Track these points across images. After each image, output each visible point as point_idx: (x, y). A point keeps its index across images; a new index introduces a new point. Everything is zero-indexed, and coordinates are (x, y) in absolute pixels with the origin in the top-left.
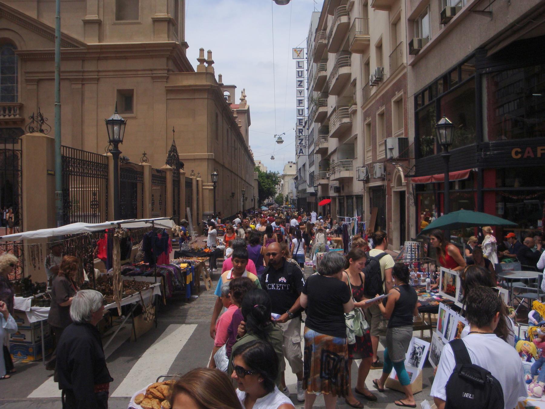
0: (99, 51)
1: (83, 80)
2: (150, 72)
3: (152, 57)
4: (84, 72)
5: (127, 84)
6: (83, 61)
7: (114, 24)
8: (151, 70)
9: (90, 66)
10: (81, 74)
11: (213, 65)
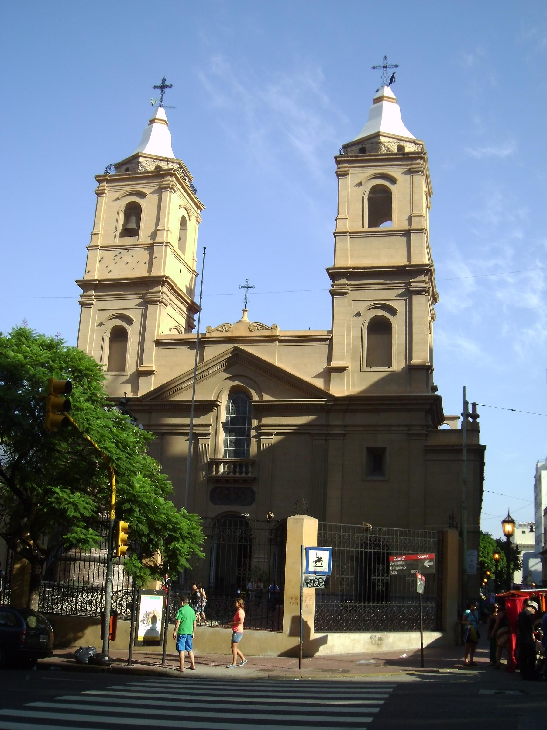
1: (327, 435)
2: (406, 428)
4: (328, 426)
8: (407, 426)
11: (478, 420)
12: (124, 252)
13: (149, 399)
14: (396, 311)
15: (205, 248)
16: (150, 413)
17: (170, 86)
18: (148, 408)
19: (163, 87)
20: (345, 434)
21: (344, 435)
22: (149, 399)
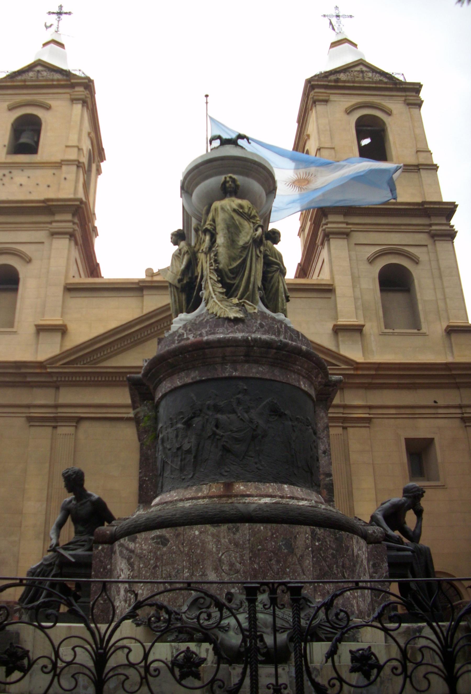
0: (373, 372)
1: (345, 420)
3: (458, 386)
7: (383, 334)
10: (341, 410)
13: (58, 365)
14: (418, 258)
15: (207, 96)
16: (57, 388)
18: (55, 379)
21: (369, 420)
22: (58, 365)
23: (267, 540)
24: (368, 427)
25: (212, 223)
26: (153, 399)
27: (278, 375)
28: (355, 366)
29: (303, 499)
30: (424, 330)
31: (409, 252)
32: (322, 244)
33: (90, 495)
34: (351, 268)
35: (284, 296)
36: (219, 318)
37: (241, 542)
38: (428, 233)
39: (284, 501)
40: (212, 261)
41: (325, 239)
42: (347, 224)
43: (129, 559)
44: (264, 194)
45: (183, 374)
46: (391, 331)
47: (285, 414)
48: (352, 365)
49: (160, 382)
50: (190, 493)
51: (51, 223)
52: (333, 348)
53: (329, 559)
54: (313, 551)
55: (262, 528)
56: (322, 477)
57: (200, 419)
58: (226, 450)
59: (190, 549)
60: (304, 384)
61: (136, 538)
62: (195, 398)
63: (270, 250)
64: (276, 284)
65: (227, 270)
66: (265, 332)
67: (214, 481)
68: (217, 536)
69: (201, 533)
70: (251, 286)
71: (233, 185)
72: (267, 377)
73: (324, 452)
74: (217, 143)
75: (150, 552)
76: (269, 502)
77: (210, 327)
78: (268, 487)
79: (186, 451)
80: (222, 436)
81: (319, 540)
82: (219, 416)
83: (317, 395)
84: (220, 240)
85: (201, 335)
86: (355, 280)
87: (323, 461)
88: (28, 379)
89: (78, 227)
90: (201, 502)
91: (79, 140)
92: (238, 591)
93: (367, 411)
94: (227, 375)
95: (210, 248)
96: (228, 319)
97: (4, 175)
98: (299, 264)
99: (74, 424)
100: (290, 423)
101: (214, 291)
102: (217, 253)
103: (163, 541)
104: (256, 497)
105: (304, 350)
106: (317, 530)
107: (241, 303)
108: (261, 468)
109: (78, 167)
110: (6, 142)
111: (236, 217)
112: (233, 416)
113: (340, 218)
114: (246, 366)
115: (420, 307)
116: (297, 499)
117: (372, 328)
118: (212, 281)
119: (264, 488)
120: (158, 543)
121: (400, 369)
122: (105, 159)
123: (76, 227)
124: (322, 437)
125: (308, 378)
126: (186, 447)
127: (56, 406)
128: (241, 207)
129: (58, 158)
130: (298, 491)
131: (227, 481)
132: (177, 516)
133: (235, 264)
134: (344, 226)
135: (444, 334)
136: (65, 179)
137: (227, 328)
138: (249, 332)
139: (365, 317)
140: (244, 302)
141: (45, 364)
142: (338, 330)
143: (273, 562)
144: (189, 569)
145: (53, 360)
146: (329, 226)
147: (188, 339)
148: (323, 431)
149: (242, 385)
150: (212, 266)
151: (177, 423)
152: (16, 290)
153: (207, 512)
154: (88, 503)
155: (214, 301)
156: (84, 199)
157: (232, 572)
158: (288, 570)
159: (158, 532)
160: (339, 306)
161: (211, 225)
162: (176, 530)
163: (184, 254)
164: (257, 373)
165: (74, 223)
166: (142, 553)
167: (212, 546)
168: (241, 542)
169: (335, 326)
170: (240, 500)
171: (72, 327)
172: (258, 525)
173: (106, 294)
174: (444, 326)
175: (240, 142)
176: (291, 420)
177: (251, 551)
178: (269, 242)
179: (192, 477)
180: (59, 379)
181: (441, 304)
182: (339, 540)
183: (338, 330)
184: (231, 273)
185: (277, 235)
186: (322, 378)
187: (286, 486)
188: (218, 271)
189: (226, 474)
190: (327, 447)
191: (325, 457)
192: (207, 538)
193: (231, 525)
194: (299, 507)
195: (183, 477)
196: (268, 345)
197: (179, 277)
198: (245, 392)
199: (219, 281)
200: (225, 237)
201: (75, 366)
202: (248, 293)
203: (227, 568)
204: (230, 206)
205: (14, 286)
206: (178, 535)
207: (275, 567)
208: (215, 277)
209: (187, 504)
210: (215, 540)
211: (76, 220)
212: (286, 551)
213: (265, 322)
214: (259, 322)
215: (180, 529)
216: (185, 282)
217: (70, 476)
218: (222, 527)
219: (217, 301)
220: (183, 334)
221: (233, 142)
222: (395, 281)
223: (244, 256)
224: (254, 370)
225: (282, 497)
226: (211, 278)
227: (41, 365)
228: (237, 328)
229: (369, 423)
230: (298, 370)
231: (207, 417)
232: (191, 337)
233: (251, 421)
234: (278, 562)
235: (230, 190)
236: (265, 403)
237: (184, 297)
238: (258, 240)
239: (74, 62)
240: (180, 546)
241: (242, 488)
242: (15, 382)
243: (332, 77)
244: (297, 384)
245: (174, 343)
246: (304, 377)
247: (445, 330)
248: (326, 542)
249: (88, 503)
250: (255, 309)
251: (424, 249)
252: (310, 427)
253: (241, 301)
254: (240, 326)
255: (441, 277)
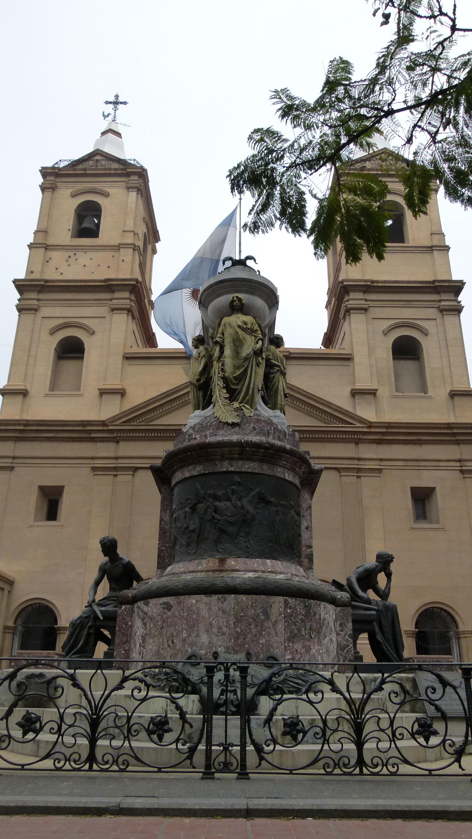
0: (384, 430)
1: (359, 470)
2: (458, 464)
4: (359, 459)
5: (425, 480)
6: (357, 443)
8: (460, 461)
9: (368, 451)
10: (356, 462)
12: (80, 255)
13: (118, 423)
14: (427, 331)
16: (118, 442)
17: (125, 103)
18: (115, 435)
19: (116, 103)
20: (381, 469)
21: (380, 470)
22: (118, 423)
23: (248, 608)
24: (379, 477)
25: (221, 336)
26: (170, 483)
27: (266, 469)
28: (369, 424)
29: (280, 573)
30: (430, 393)
31: (418, 325)
32: (344, 318)
33: (121, 559)
34: (368, 339)
35: (282, 393)
36: (220, 422)
37: (228, 610)
38: (438, 308)
39: (264, 575)
40: (220, 370)
41: (347, 314)
42: (366, 300)
43: (143, 620)
44: (267, 308)
45: (191, 467)
46: (401, 394)
47: (271, 502)
48: (366, 424)
49: (174, 472)
50: (192, 566)
51: (111, 300)
52: (350, 409)
53: (298, 624)
54: (285, 617)
55: (244, 598)
56: (304, 548)
57: (203, 505)
58: (222, 531)
59: (188, 614)
60: (289, 475)
61: (149, 602)
62: (199, 487)
63: (272, 354)
64: (277, 384)
65: (231, 377)
66: (258, 434)
67: (212, 556)
68: (209, 604)
69: (197, 601)
70: (250, 392)
71: (239, 304)
72: (257, 471)
73: (307, 528)
74: (229, 263)
75: (159, 615)
76: (252, 576)
77: (213, 430)
78: (254, 562)
79: (191, 531)
80: (219, 520)
81: (290, 608)
82: (217, 503)
83: (301, 483)
84: (228, 352)
85: (205, 436)
86: (371, 350)
87: (305, 535)
88: (93, 435)
89: (135, 304)
90: (199, 575)
91: (135, 225)
92: (224, 650)
93: (378, 463)
94: (225, 470)
95: (219, 358)
96: (227, 423)
97: (70, 257)
98: (325, 334)
99: (132, 473)
100: (275, 509)
101: (220, 395)
102: (224, 363)
103: (168, 607)
104: (242, 571)
105: (288, 449)
106: (289, 600)
107: (241, 407)
108: (249, 546)
109: (134, 250)
110: (71, 228)
111: (240, 332)
112: (228, 504)
113: (360, 295)
114: (240, 463)
115: (428, 373)
116: (276, 573)
117: (384, 392)
118: (219, 387)
119: (250, 564)
120: (164, 608)
121: (407, 428)
122: (160, 240)
123: (134, 305)
124: (305, 515)
125: (292, 469)
126: (192, 527)
127: (116, 458)
128: (245, 323)
129: (116, 242)
130: (279, 565)
131: (222, 556)
132: (180, 587)
133: (238, 372)
134: (363, 302)
135: (448, 397)
136: (123, 260)
137: (226, 431)
138: (244, 434)
139: (378, 382)
140: (244, 406)
141: (106, 422)
142: (355, 393)
143: (252, 626)
144: (187, 631)
145: (114, 419)
146: (351, 302)
147: (196, 438)
148: (307, 511)
149: (237, 478)
150: (219, 374)
151: (185, 507)
152: (82, 358)
153: (202, 584)
154: (120, 565)
155: (219, 405)
156: (140, 279)
157: (219, 634)
158: (264, 633)
159: (164, 600)
160: (356, 373)
161: (220, 338)
162: (178, 598)
163: (202, 358)
164: (249, 468)
165: (131, 300)
166: (152, 616)
167: (204, 613)
168: (228, 610)
169: (352, 390)
170: (229, 574)
171: (129, 391)
172: (242, 596)
173: (159, 362)
174: (448, 392)
175: (249, 263)
176: (276, 506)
177: (236, 618)
178: (273, 347)
179: (195, 552)
180: (119, 435)
181: (447, 371)
182: (308, 607)
183: (355, 393)
184: (235, 380)
185: (280, 340)
186: (305, 469)
187: (268, 561)
188: (225, 379)
189: (221, 551)
190: (309, 524)
191: (307, 532)
192: (202, 606)
193: (220, 596)
194: (276, 581)
195: (189, 552)
196: (258, 446)
197: (197, 377)
198: (239, 484)
199: (224, 387)
200: (231, 349)
201: (132, 424)
202: (248, 397)
203: (216, 631)
204: (236, 322)
205: (80, 355)
206: (179, 603)
207: (254, 631)
208: (221, 384)
209: (189, 577)
210: (207, 608)
211: (133, 298)
212: (263, 617)
213: (257, 426)
214: (252, 426)
215: (182, 598)
216: (202, 382)
217: (105, 543)
218: (213, 597)
219: (221, 406)
220: (192, 434)
221: (242, 263)
222: (406, 350)
223: (246, 365)
224: (246, 466)
225: (263, 572)
226: (218, 384)
227: (103, 423)
228: (234, 431)
229: (379, 473)
230: (284, 464)
231: (208, 504)
232: (198, 437)
233: (243, 507)
234: (256, 626)
235: (237, 308)
236: (254, 493)
237: (201, 394)
238: (258, 352)
239: (129, 150)
240: (181, 612)
241: (232, 563)
242: (81, 438)
243: (358, 166)
244: (282, 476)
245: (185, 441)
246: (289, 469)
247: (449, 394)
248: (296, 609)
249: (120, 565)
250: (251, 412)
251: (434, 322)
252: (293, 510)
253: (241, 405)
254: (237, 429)
255: (447, 347)
